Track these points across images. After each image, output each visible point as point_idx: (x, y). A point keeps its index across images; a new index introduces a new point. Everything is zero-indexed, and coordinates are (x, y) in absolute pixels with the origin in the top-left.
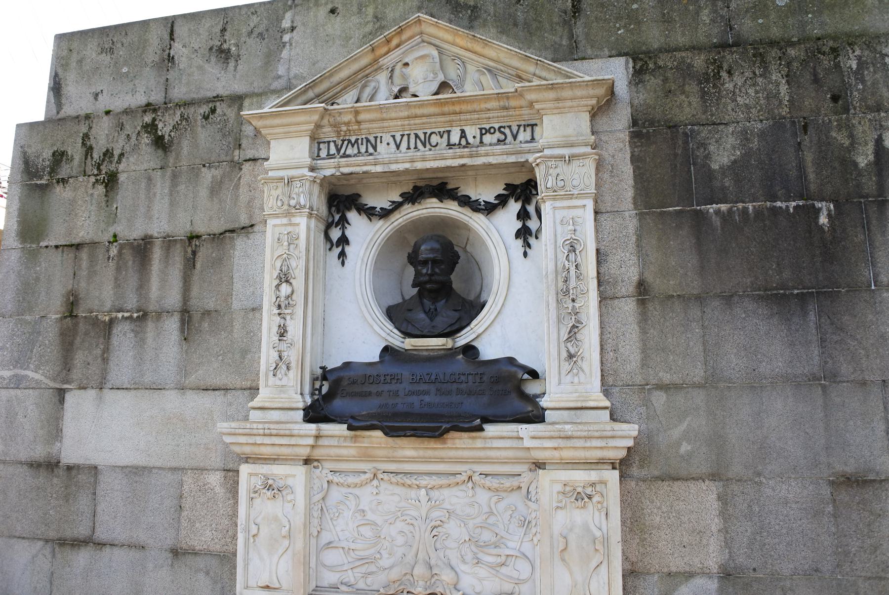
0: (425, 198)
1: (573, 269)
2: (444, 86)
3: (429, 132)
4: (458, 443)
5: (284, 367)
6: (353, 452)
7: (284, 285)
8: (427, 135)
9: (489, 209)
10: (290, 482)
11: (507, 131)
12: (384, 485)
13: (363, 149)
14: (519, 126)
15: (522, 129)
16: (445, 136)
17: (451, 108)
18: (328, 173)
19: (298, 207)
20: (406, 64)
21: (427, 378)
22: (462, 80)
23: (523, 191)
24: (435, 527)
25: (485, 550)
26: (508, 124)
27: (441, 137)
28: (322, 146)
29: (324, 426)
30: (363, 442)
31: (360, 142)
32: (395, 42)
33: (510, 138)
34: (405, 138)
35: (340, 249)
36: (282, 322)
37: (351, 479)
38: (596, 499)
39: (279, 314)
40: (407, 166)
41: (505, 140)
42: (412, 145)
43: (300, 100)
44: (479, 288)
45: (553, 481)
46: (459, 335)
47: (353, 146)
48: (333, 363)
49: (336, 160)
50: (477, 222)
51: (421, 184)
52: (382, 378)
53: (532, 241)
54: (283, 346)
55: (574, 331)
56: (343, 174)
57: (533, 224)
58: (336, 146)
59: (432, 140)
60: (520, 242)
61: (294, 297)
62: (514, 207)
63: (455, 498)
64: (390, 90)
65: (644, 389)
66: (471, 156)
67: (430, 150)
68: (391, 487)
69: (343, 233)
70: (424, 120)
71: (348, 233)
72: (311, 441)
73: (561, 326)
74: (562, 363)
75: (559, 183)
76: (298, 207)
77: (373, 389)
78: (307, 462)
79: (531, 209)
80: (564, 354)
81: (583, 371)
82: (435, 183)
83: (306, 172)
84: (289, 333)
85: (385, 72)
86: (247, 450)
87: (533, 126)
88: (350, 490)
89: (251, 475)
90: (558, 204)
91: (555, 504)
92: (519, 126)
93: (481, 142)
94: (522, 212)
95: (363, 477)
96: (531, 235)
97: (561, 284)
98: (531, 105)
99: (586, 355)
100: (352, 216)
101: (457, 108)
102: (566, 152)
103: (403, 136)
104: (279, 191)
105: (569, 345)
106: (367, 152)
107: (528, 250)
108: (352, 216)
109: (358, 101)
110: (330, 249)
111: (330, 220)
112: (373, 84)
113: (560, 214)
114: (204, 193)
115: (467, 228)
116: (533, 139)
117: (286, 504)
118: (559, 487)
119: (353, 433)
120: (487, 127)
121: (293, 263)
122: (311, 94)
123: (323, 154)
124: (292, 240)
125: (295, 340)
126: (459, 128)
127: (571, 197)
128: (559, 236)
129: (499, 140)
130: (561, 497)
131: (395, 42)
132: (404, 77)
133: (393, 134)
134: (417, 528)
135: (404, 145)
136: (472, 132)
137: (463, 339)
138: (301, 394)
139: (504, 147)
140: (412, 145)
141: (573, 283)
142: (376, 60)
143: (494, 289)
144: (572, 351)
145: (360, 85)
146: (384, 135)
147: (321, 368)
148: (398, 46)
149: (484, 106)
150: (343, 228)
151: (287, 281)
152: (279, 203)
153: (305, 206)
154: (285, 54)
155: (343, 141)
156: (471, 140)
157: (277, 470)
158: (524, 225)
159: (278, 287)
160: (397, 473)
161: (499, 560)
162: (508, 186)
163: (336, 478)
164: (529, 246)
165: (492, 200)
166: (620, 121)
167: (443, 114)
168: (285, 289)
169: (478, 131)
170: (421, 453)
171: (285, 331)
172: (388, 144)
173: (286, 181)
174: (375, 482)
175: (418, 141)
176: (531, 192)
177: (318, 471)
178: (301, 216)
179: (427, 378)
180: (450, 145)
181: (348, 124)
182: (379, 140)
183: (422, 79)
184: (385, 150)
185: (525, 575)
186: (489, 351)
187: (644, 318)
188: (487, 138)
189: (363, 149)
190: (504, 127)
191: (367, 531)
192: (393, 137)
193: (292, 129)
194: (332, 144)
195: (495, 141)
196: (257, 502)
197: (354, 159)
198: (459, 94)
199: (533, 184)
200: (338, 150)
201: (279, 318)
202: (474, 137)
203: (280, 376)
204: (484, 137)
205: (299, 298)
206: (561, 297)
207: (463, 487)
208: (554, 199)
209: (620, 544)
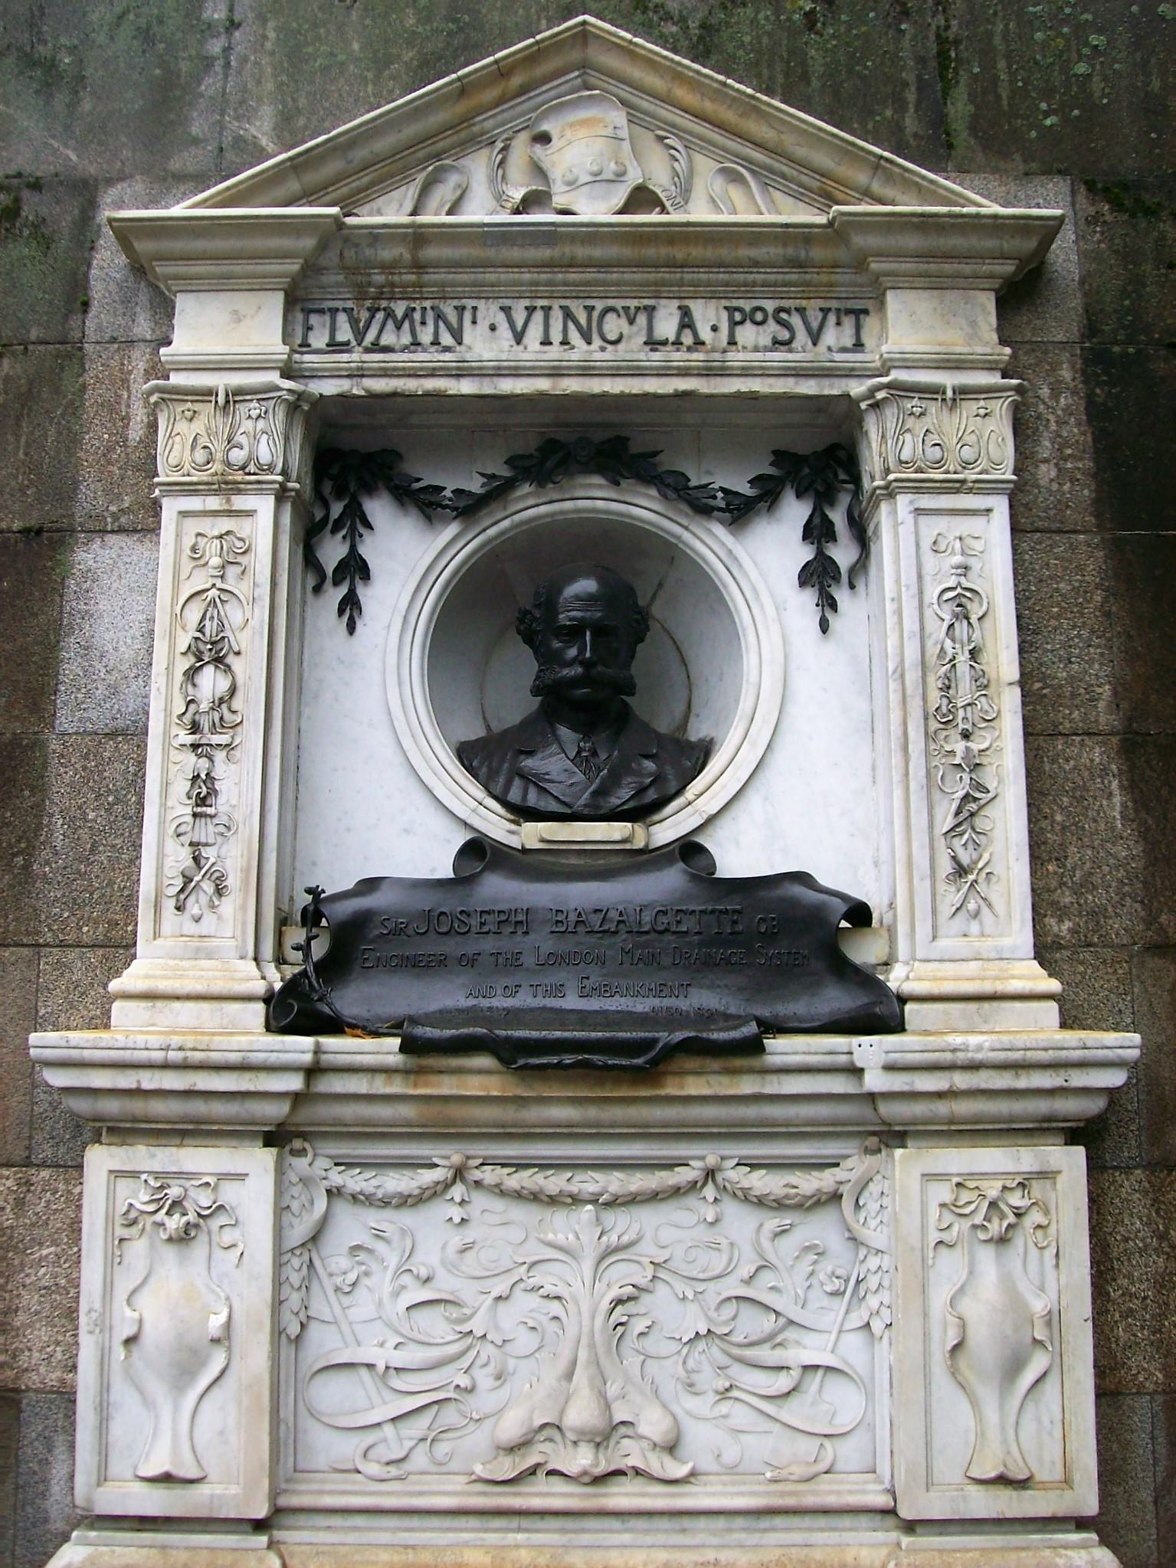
0: (570, 474)
1: (963, 658)
2: (642, 198)
3: (600, 305)
4: (694, 1087)
5: (208, 887)
6: (407, 1111)
7: (209, 671)
8: (596, 314)
9: (739, 512)
10: (230, 1193)
11: (796, 320)
12: (480, 1201)
13: (426, 336)
14: (825, 311)
15: (832, 318)
16: (642, 319)
17: (664, 251)
18: (329, 388)
19: (252, 468)
20: (544, 139)
21: (595, 920)
22: (685, 191)
24: (619, 1302)
25: (748, 1353)
26: (797, 303)
27: (631, 322)
28: (314, 319)
29: (329, 1042)
30: (440, 1085)
31: (417, 316)
32: (516, 81)
33: (802, 337)
34: (538, 316)
35: (343, 590)
36: (204, 763)
37: (395, 1182)
38: (1035, 1217)
39: (195, 747)
40: (543, 385)
41: (789, 342)
42: (556, 336)
43: (281, 192)
44: (679, 709)
45: (929, 1177)
46: (656, 817)
47: (399, 327)
48: (337, 879)
49: (355, 356)
51: (562, 435)
52: (474, 922)
53: (841, 595)
54: (205, 831)
55: (970, 810)
56: (372, 396)
57: (843, 554)
58: (354, 322)
59: (606, 327)
60: (809, 598)
61: (236, 704)
62: (795, 512)
64: (500, 198)
66: (708, 372)
67: (603, 349)
68: (498, 1204)
69: (353, 548)
70: (590, 275)
71: (368, 550)
72: (294, 1083)
73: (937, 795)
74: (942, 887)
75: (929, 451)
76: (252, 468)
77: (451, 947)
78: (270, 1139)
79: (838, 517)
80: (946, 867)
81: (990, 906)
82: (599, 436)
83: (274, 377)
84: (222, 799)
85: (485, 152)
86: (111, 1107)
87: (858, 314)
88: (388, 1214)
89: (117, 1174)
90: (927, 501)
91: (934, 1236)
92: (825, 311)
93: (732, 342)
94: (817, 521)
95: (428, 1177)
96: (836, 577)
97: (935, 697)
98: (860, 264)
99: (997, 868)
100: (379, 509)
101: (679, 253)
102: (948, 380)
103: (531, 310)
104: (198, 426)
105: (957, 843)
106: (436, 342)
107: (829, 615)
108: (379, 509)
109: (414, 213)
110: (317, 589)
111: (319, 515)
112: (453, 179)
113: (932, 527)
115: (671, 554)
116: (859, 346)
117: (218, 1253)
118: (943, 1192)
119: (412, 1061)
120: (747, 305)
121: (234, 614)
122: (294, 186)
123: (319, 340)
124: (235, 556)
125: (238, 816)
126: (676, 303)
127: (958, 487)
128: (927, 579)
129: (776, 342)
130: (948, 1218)
131: (516, 81)
132: (539, 171)
133: (507, 302)
134: (571, 1307)
135: (534, 333)
137: (667, 830)
138: (256, 959)
139: (790, 356)
140: (556, 336)
141: (964, 690)
142: (467, 119)
143: (745, 705)
144: (965, 859)
145: (421, 177)
146: (481, 304)
147: (309, 891)
148: (523, 90)
149: (745, 252)
150: (353, 538)
151: (218, 661)
152: (200, 456)
153: (270, 468)
154: (210, 85)
155: (373, 311)
156: (705, 334)
157: (201, 1159)
158: (820, 554)
159: (191, 674)
160: (520, 1167)
161: (782, 1382)
162: (780, 457)
163: (355, 1181)
164: (833, 606)
165: (745, 489)
166: (1061, 323)
167: (641, 264)
168: (211, 683)
169: (725, 315)
170: (593, 1112)
171: (213, 792)
172: (493, 328)
173: (221, 399)
174: (458, 1191)
175: (571, 325)
176: (836, 475)
177: (301, 1164)
178: (260, 492)
179: (595, 920)
180: (653, 344)
181: (388, 267)
182: (467, 316)
185: (845, 1420)
186: (738, 856)
188: (747, 334)
189: (426, 336)
190: (788, 311)
191: (435, 1325)
192: (506, 310)
193: (237, 268)
194: (342, 318)
195: (765, 340)
196: (138, 1249)
197: (405, 356)
198: (675, 217)
199: (842, 454)
200: (360, 335)
201: (193, 757)
202: (714, 329)
203: (196, 911)
204: (739, 329)
205: (250, 706)
206: (934, 725)
207: (691, 1201)
208: (918, 491)
209: (1090, 1324)
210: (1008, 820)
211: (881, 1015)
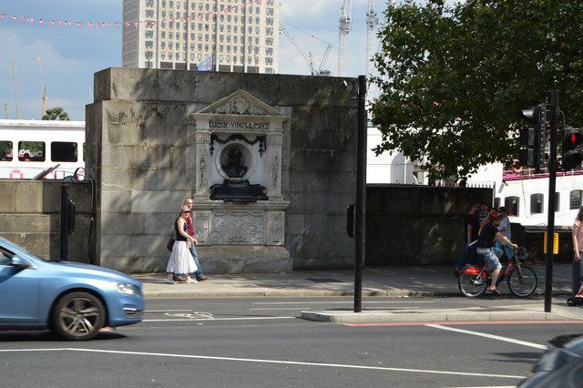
9: (252, 143)
23: (262, 139)
50: (249, 146)
57: (263, 148)
62: (258, 143)
63: (246, 219)
65: (290, 193)
114: (175, 132)
115: (246, 148)
136: (252, 124)
137: (244, 178)
183: (241, 107)
184: (229, 127)
186: (252, 182)
187: (290, 176)
210: (279, 179)
211: (266, 199)
